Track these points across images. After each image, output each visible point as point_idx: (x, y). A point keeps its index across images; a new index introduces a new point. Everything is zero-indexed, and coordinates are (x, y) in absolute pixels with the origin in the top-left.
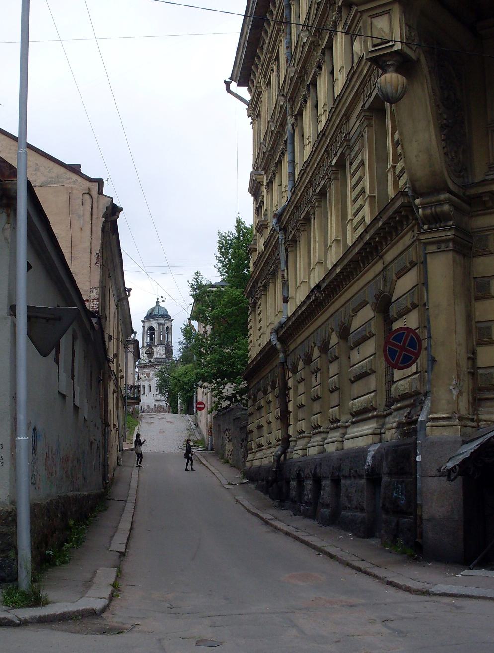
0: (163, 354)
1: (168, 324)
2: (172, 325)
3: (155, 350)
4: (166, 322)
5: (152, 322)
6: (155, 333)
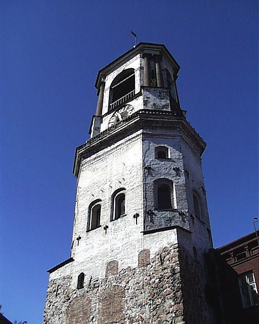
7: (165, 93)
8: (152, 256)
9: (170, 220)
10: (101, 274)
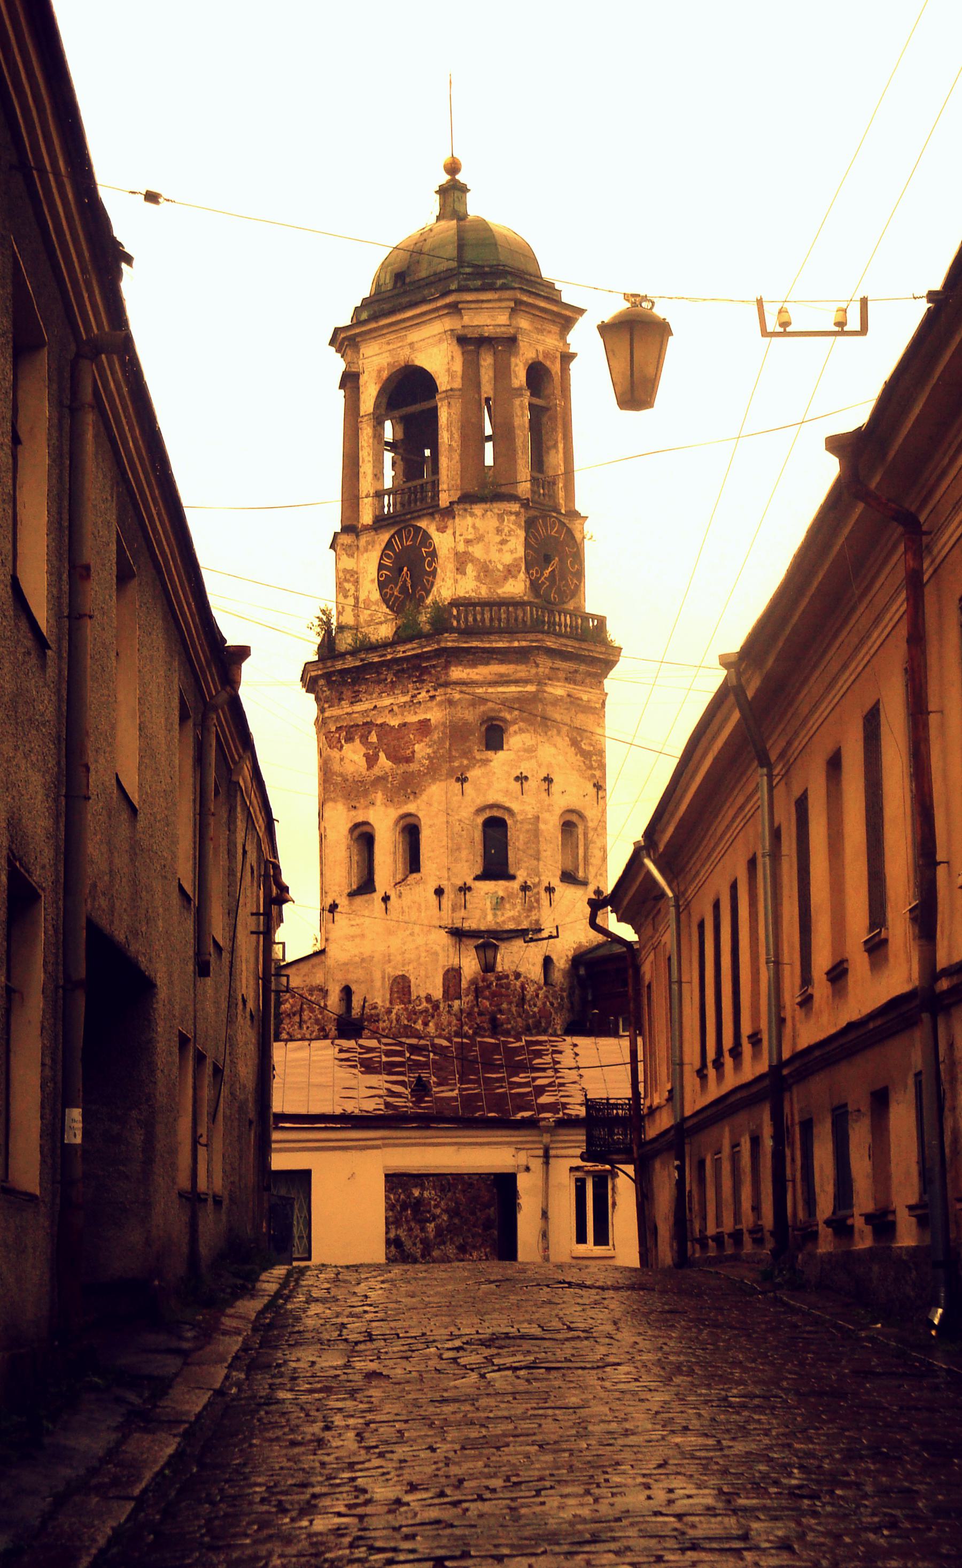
0: (510, 572)
1: (535, 344)
2: (567, 358)
3: (443, 541)
4: (524, 323)
5: (414, 336)
6: (443, 416)
7: (513, 518)
8: (464, 985)
9: (499, 903)
10: (380, 998)
